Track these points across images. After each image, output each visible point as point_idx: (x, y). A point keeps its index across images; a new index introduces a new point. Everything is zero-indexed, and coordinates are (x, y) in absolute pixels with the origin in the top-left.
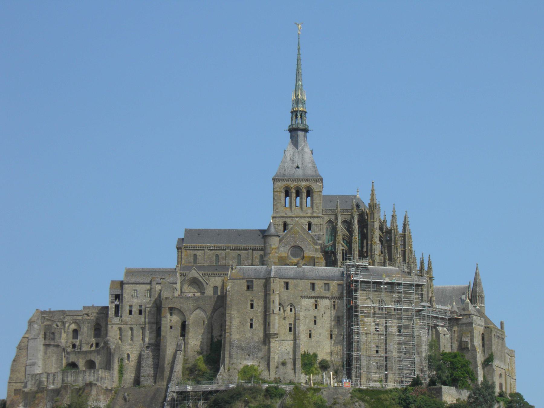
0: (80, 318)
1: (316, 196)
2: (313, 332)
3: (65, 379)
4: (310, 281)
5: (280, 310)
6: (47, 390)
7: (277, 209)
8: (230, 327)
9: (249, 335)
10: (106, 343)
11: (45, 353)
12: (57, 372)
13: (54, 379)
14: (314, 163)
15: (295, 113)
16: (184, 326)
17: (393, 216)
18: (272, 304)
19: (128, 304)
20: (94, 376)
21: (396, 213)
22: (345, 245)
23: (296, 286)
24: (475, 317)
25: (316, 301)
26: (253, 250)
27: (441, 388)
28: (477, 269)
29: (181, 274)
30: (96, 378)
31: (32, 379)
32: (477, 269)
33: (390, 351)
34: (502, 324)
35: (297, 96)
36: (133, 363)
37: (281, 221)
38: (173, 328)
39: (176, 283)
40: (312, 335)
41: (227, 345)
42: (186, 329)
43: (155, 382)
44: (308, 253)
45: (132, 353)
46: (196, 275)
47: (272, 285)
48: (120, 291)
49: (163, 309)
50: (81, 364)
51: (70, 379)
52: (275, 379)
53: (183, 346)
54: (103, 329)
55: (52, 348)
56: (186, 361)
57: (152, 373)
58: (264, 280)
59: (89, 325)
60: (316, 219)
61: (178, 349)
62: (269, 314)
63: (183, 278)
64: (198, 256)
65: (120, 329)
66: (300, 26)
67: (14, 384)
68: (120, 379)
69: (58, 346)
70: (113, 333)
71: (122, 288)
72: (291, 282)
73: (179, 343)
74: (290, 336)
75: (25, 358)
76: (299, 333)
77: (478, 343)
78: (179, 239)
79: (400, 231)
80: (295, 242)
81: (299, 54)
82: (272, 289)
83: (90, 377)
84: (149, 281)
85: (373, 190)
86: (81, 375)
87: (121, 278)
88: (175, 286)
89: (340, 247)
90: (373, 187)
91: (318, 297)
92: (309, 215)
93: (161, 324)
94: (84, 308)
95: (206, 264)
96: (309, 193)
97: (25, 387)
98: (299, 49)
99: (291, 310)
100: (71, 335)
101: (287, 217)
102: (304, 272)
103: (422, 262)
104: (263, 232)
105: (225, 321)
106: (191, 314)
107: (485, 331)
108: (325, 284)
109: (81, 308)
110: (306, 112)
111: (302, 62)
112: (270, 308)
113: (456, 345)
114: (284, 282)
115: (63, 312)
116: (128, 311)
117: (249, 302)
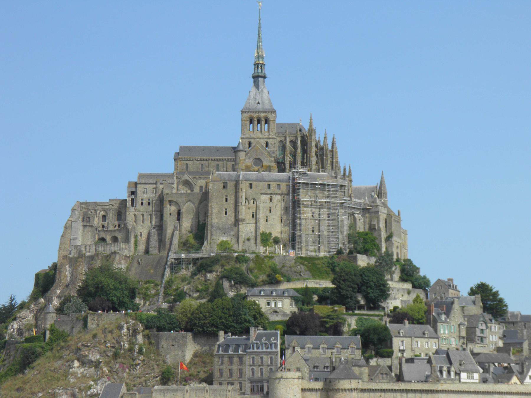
0: (107, 207)
1: (271, 123)
2: (269, 218)
3: (97, 249)
5: (246, 203)
6: (85, 256)
7: (244, 132)
8: (211, 214)
9: (224, 220)
10: (125, 225)
11: (84, 231)
12: (92, 244)
13: (90, 249)
14: (270, 100)
15: (257, 65)
16: (179, 213)
17: (325, 138)
18: (240, 198)
19: (141, 198)
20: (117, 247)
22: (291, 158)
23: (257, 186)
24: (380, 207)
25: (271, 197)
26: (227, 161)
27: (356, 256)
28: (382, 174)
29: (177, 178)
30: (118, 248)
32: (382, 174)
33: (322, 231)
34: (399, 212)
35: (258, 53)
36: (144, 238)
37: (247, 141)
39: (174, 184)
40: (268, 220)
41: (209, 227)
42: (181, 215)
43: (159, 252)
44: (266, 163)
45: (143, 231)
46: (188, 178)
47: (240, 185)
49: (165, 202)
50: (108, 239)
51: (101, 249)
52: (243, 250)
53: (179, 227)
54: (123, 215)
55: (88, 228)
56: (180, 237)
57: (157, 246)
58: (235, 182)
59: (114, 212)
60: (271, 140)
61: (175, 229)
62: (239, 206)
63: (179, 180)
64: (189, 165)
65: (135, 215)
66: (260, 4)
67: (62, 252)
68: (135, 249)
69: (92, 226)
70: (130, 218)
71: (136, 187)
72: (254, 184)
73: (176, 225)
74: (253, 221)
75: (70, 234)
76: (259, 219)
77: (382, 225)
78: (176, 153)
79: (330, 148)
80: (257, 156)
81: (260, 24)
82: (240, 188)
83: (114, 248)
84: (155, 182)
85: (311, 120)
86: (109, 246)
87: (136, 180)
88: (173, 185)
89: (288, 159)
90: (311, 117)
91: (272, 194)
92: (266, 136)
94: (110, 200)
95: (195, 171)
96: (267, 121)
97: (70, 254)
98: (260, 20)
100: (101, 219)
101: (251, 138)
102: (262, 176)
103: (345, 170)
104: (234, 148)
105: (208, 210)
106: (184, 205)
107: (387, 217)
108: (278, 185)
109: (108, 201)
110: (264, 65)
111: (262, 29)
112: (239, 201)
113: (367, 227)
114: (249, 183)
115: (96, 203)
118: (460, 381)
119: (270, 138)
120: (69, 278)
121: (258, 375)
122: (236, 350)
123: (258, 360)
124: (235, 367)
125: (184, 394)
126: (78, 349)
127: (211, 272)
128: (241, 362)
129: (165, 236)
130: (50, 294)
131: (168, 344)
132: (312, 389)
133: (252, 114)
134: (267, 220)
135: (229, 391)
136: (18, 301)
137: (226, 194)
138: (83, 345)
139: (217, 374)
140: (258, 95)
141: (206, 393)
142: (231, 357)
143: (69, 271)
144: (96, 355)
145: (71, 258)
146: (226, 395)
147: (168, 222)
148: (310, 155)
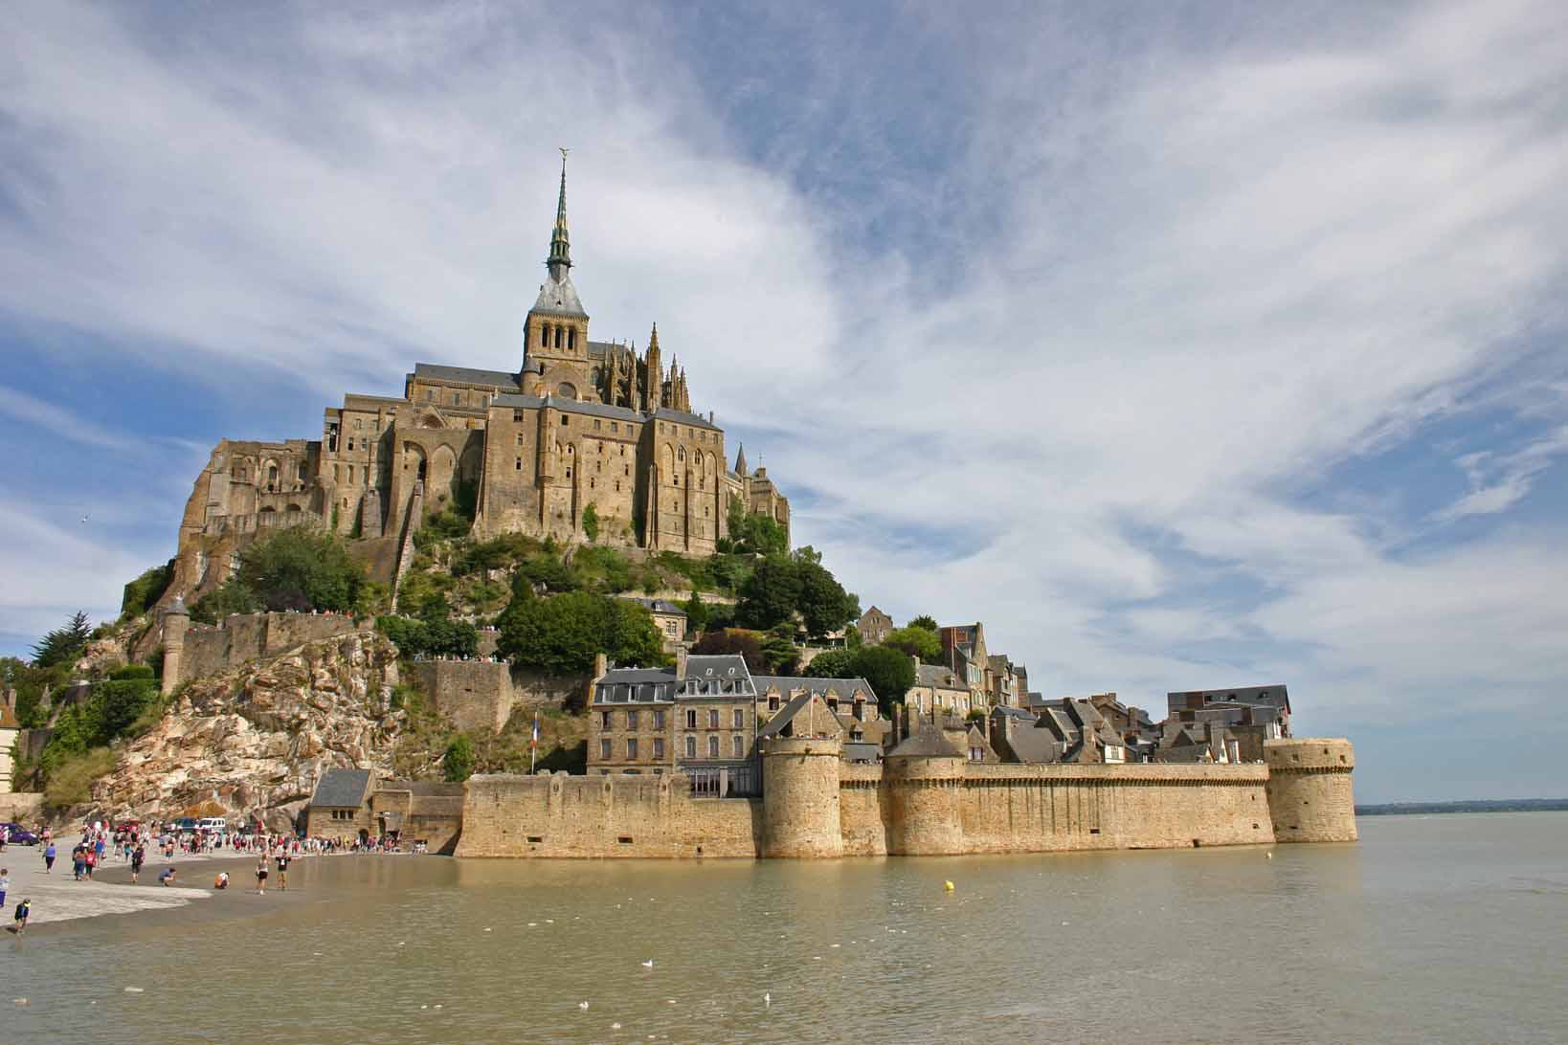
0: (281, 453)
4: (594, 418)
8: (491, 464)
10: (317, 483)
11: (233, 493)
21: (677, 363)
23: (577, 421)
25: (601, 443)
31: (214, 523)
38: (409, 467)
40: (595, 484)
46: (434, 413)
47: (548, 416)
48: (339, 419)
70: (326, 470)
71: (341, 417)
73: (417, 488)
76: (580, 480)
85: (654, 332)
91: (604, 439)
92: (572, 358)
93: (392, 463)
95: (444, 404)
96: (573, 333)
97: (205, 531)
98: (563, 175)
99: (570, 451)
107: (779, 504)
108: (613, 423)
115: (258, 445)
116: (347, 445)
117: (517, 436)
118: (1103, 760)
119: (577, 361)
120: (200, 577)
121: (704, 752)
122: (647, 695)
123: (703, 718)
124: (645, 736)
125: (549, 796)
126: (246, 694)
127: (496, 567)
128: (661, 727)
129: (396, 505)
130: (162, 603)
131: (458, 686)
132: (858, 782)
133: (549, 319)
134: (592, 484)
135: (664, 788)
136: (93, 623)
137: (519, 431)
138: (258, 682)
139: (595, 751)
140: (558, 290)
141: (604, 792)
142: (633, 711)
143: (202, 562)
144: (291, 706)
145: (209, 538)
146: (658, 797)
147: (402, 479)
148: (652, 389)
